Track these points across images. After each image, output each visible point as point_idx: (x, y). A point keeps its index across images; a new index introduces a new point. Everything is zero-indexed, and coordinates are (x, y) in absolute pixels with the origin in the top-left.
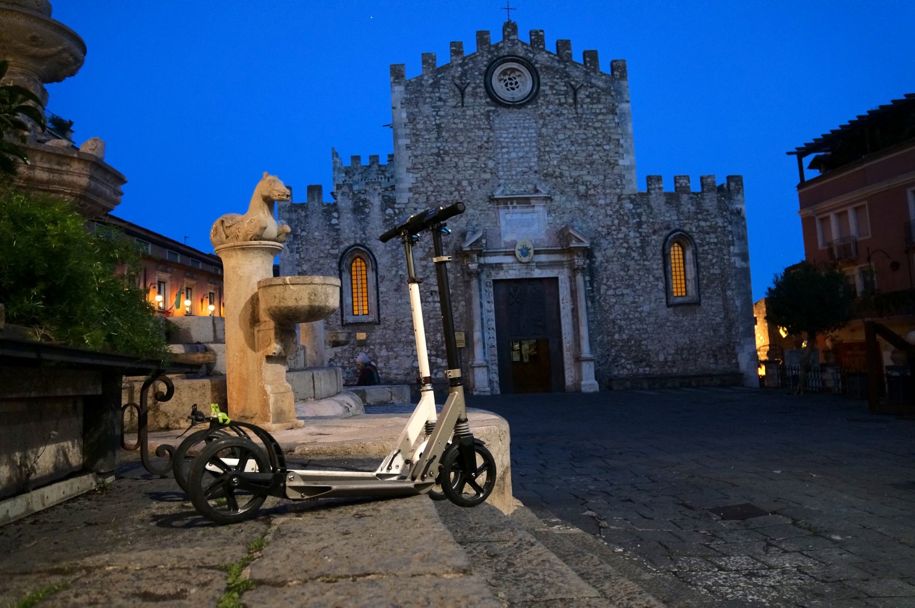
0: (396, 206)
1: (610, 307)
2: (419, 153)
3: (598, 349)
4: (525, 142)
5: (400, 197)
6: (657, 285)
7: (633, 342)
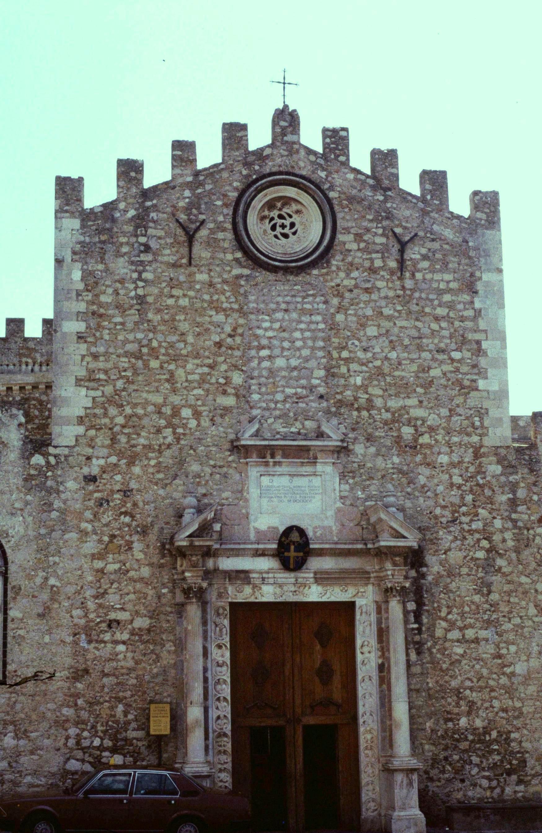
0: (51, 450)
1: (452, 664)
2: (102, 349)
3: (427, 747)
4: (304, 339)
7: (494, 734)
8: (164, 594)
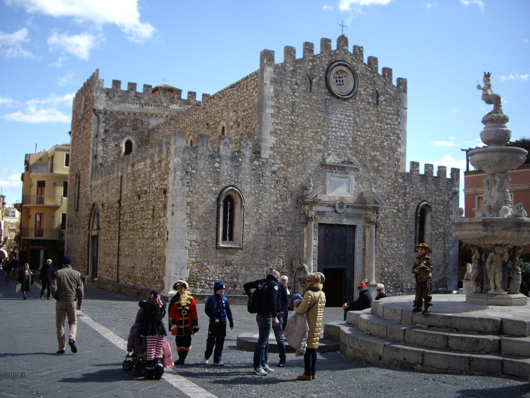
0: (261, 159)
1: (384, 249)
4: (346, 125)
5: (264, 153)
6: (411, 237)
8: (297, 218)
